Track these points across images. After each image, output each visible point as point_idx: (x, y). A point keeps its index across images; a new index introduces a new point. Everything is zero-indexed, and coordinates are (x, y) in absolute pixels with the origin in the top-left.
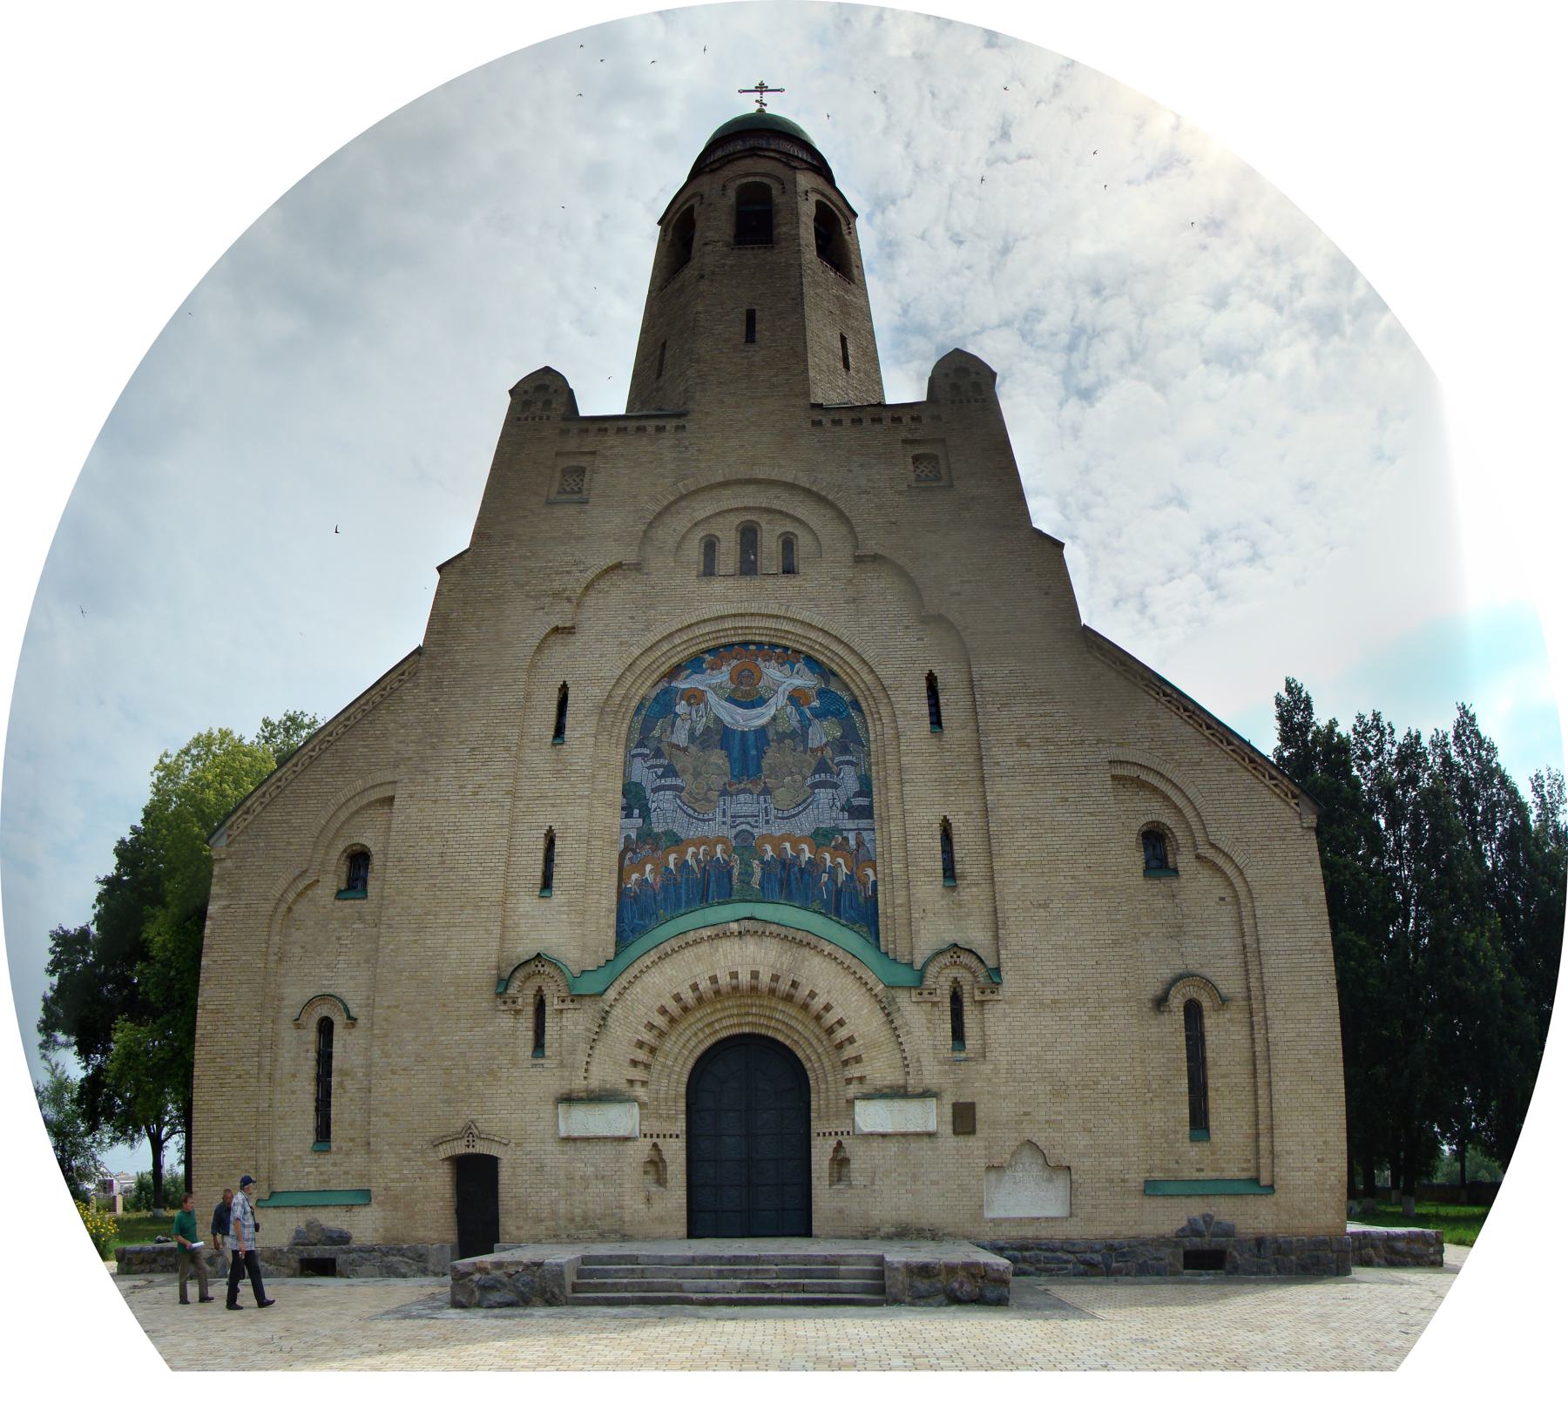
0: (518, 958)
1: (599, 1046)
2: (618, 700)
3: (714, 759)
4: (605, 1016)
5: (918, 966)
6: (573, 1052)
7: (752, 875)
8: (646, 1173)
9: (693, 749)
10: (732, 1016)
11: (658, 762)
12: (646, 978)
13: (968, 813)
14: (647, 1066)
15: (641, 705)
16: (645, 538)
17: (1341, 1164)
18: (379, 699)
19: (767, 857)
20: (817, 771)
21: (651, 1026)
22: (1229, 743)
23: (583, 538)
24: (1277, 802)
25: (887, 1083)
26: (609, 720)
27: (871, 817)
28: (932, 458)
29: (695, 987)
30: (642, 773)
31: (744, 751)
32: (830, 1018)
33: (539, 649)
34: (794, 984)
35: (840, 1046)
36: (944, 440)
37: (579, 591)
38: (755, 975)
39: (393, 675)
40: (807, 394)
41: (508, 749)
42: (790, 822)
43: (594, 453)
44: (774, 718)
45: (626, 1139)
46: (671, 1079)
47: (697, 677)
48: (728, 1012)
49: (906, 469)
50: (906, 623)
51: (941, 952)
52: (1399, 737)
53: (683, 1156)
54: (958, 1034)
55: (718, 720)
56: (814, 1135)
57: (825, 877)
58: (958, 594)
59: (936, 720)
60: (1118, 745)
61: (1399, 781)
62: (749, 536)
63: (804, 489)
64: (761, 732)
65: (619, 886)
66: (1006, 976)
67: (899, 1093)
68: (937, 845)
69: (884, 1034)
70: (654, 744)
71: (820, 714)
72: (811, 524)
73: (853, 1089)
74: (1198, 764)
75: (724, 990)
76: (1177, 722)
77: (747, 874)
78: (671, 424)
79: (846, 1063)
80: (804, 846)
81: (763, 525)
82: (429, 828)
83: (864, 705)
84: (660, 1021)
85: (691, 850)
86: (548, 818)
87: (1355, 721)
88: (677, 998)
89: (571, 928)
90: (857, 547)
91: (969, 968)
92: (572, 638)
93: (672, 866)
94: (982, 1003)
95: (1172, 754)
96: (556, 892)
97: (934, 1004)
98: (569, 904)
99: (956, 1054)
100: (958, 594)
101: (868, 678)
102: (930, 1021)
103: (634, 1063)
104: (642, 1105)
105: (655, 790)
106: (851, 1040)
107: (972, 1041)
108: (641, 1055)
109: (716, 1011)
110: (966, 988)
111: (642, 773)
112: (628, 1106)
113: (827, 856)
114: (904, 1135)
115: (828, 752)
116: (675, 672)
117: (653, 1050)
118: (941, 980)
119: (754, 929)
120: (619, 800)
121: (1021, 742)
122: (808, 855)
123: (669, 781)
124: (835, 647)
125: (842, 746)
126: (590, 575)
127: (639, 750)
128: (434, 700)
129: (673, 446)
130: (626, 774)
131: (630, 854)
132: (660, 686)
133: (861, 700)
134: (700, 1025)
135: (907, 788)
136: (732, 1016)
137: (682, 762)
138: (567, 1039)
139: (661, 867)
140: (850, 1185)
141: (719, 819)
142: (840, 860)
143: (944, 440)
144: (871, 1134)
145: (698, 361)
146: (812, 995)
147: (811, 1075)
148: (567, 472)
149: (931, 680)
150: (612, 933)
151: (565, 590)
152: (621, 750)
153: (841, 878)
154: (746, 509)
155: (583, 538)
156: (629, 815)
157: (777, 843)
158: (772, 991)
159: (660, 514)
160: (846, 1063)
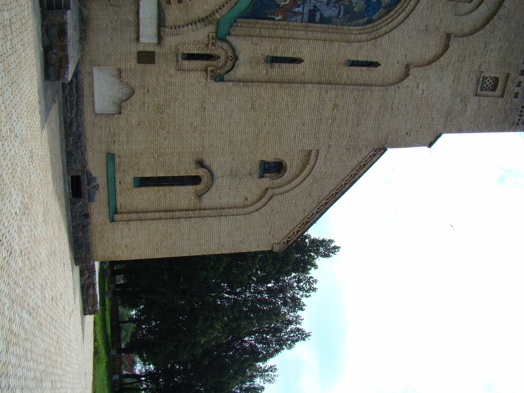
13: (304, 74)
17: (125, 257)
22: (317, 213)
24: (286, 233)
25: (167, 16)
28: (494, 88)
36: (502, 96)
49: (492, 74)
50: (408, 56)
51: (234, 51)
52: (304, 300)
54: (191, 57)
58: (417, 87)
59: (354, 64)
61: (286, 296)
66: (219, 85)
67: (161, 23)
68: (290, 55)
74: (310, 195)
76: (331, 188)
83: (369, 26)
87: (315, 278)
90: (456, 36)
91: (224, 65)
94: (206, 71)
95: (317, 183)
97: (207, 45)
99: (180, 55)
100: (417, 87)
101: (383, 31)
102: (199, 42)
110: (214, 63)
114: (138, 24)
118: (219, 50)
121: (336, 106)
125: (349, 10)
135: (321, 43)
143: (502, 96)
144: (138, 6)
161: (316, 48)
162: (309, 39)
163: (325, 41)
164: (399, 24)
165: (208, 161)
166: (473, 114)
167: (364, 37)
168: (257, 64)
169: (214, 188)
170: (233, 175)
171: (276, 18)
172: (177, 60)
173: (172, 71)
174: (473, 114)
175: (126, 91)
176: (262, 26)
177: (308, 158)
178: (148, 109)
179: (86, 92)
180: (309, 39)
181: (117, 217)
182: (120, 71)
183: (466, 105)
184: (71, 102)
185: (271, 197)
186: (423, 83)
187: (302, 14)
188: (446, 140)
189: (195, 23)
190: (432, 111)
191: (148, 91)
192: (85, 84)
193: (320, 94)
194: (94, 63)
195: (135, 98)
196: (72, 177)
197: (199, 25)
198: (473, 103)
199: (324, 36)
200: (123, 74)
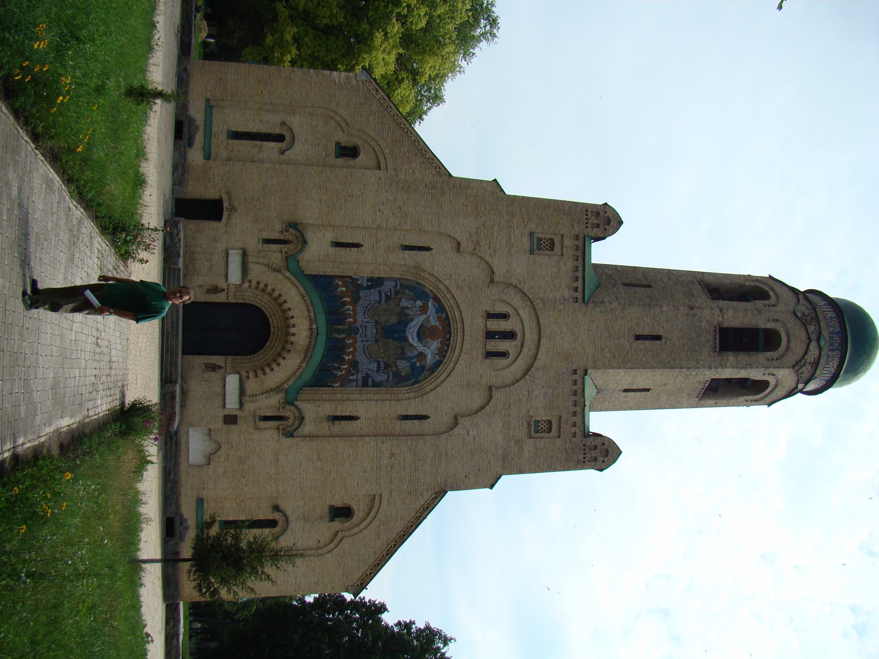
1: (266, 268)
2: (423, 274)
3: (393, 318)
4: (279, 271)
5: (295, 403)
9: (398, 309)
14: (257, 288)
15: (421, 285)
16: (508, 285)
18: (427, 156)
20: (385, 363)
21: (273, 290)
22: (387, 554)
26: (413, 271)
28: (550, 432)
29: (289, 309)
30: (388, 286)
32: (274, 366)
33: (449, 236)
35: (262, 369)
37: (479, 254)
38: (294, 335)
40: (595, 367)
41: (399, 224)
42: (361, 351)
44: (412, 345)
45: (227, 278)
46: (251, 297)
47: (434, 311)
49: (542, 416)
53: (219, 301)
54: (266, 418)
55: (412, 320)
57: (336, 365)
59: (406, 418)
60: (389, 500)
62: (510, 335)
63: (533, 364)
64: (406, 340)
66: (288, 441)
67: (242, 392)
68: (347, 414)
71: (413, 366)
73: (244, 374)
76: (398, 530)
77: (339, 331)
78: (579, 295)
79: (255, 371)
82: (365, 189)
84: (276, 294)
85: (351, 308)
88: (285, 302)
90: (498, 388)
91: (293, 424)
94: (278, 429)
96: (334, 249)
97: (279, 409)
103: (258, 283)
104: (241, 285)
105: (380, 292)
106: (265, 374)
107: (262, 424)
108: (262, 286)
110: (285, 423)
111: (388, 286)
114: (224, 395)
115: (394, 369)
116: (437, 299)
117: (264, 290)
119: (313, 335)
120: (376, 276)
121: (392, 455)
123: (383, 298)
124: (445, 374)
126: (488, 259)
130: (388, 279)
133: (418, 385)
135: (374, 402)
140: (204, 372)
141: (365, 320)
144: (225, 381)
145: (623, 308)
146: (284, 358)
148: (552, 242)
149: (426, 417)
150: (315, 273)
154: (524, 334)
156: (368, 280)
157: (353, 345)
158: (286, 342)
159: (522, 292)
160: (255, 371)
161: (369, 407)
163: (377, 400)
165: (283, 506)
168: (321, 422)
169: (288, 532)
170: (306, 518)
173: (251, 430)
176: (324, 392)
177: (373, 502)
179: (183, 447)
182: (210, 430)
183: (522, 448)
185: (342, 539)
187: (357, 380)
188: (505, 480)
197: (271, 393)
198: (528, 446)
199: (376, 397)
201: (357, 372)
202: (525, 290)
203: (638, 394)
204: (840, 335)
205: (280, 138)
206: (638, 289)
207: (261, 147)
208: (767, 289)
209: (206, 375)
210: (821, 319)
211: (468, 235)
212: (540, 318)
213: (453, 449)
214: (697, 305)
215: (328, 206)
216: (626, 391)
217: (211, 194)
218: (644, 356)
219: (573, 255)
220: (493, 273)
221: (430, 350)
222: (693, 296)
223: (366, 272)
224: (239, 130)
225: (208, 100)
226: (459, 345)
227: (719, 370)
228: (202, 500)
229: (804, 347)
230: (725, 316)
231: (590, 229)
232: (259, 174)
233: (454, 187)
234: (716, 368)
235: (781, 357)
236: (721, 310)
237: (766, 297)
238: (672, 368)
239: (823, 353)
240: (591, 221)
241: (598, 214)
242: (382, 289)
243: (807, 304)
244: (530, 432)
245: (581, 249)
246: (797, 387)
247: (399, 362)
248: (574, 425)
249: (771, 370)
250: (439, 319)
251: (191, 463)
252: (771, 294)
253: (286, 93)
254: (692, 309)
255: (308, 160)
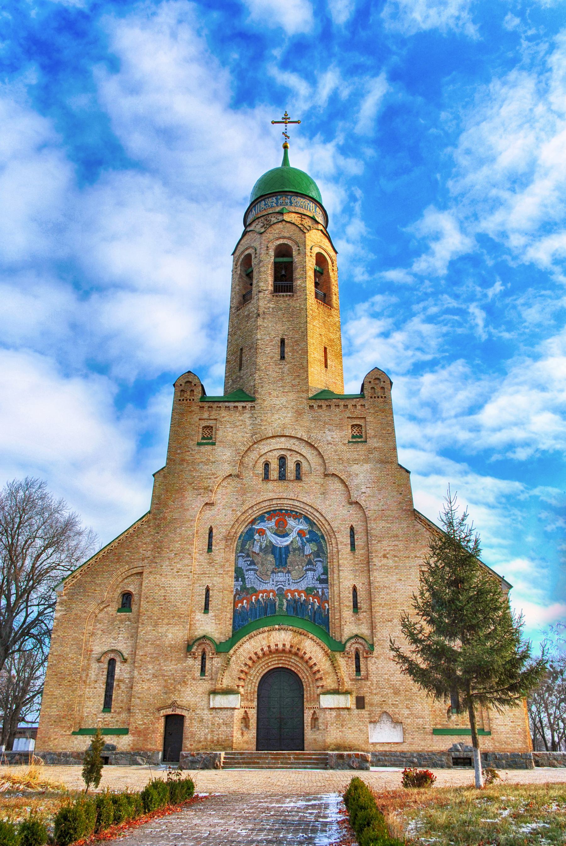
0: (195, 637)
5: (343, 643)
6: (217, 674)
7: (283, 605)
8: (242, 723)
9: (261, 554)
10: (275, 660)
11: (248, 559)
12: (244, 645)
13: (363, 584)
16: (241, 463)
19: (289, 598)
21: (246, 664)
23: (214, 462)
26: (229, 543)
27: (327, 583)
28: (361, 426)
30: (242, 563)
31: (281, 556)
34: (298, 649)
35: (315, 673)
39: (139, 523)
41: (190, 554)
43: (216, 419)
44: (292, 542)
47: (262, 524)
48: (274, 659)
49: (348, 432)
50: (343, 504)
53: (256, 716)
56: (305, 708)
57: (310, 607)
58: (365, 493)
62: (282, 460)
64: (287, 547)
65: (234, 609)
67: (336, 692)
68: (351, 596)
69: (330, 669)
70: (246, 552)
71: (309, 541)
72: (307, 457)
73: (319, 690)
75: (272, 651)
77: (281, 605)
78: (249, 405)
79: (317, 680)
80: (302, 594)
81: (289, 458)
82: (159, 585)
83: (326, 538)
85: (261, 595)
86: (207, 582)
89: (214, 626)
92: (213, 508)
93: (253, 601)
94: (367, 658)
97: (349, 658)
98: (215, 616)
99: (357, 677)
100: (365, 493)
101: (328, 527)
102: (347, 664)
103: (240, 679)
104: (242, 695)
105: (247, 570)
106: (319, 671)
108: (243, 676)
109: (269, 658)
111: (242, 563)
112: (237, 696)
113: (311, 598)
114: (338, 708)
115: (312, 556)
116: (253, 522)
118: (351, 647)
120: (234, 574)
121: (385, 556)
122: (303, 598)
124: (315, 513)
125: (317, 554)
127: (241, 554)
128: (158, 533)
129: (250, 417)
130: (236, 564)
131: (238, 596)
132: (248, 527)
134: (264, 664)
135: (341, 573)
136: (275, 660)
137: (257, 559)
138: (214, 669)
139: (249, 601)
140: (318, 729)
141: (271, 582)
142: (316, 600)
144: (326, 708)
145: (259, 370)
146: (305, 653)
147: (304, 684)
148: (205, 427)
149: (352, 529)
150: (231, 627)
151: (209, 486)
152: (234, 554)
153: (316, 607)
155: (214, 462)
156: (237, 580)
157: (292, 592)
158: (290, 651)
160: (317, 680)
162: (339, 582)
163: (339, 571)
164: (322, 515)
166: (380, 440)
167: (333, 541)
168: (359, 620)
171: (327, 607)
172: (361, 679)
173: (369, 683)
174: (380, 440)
175: (385, 717)
178: (397, 701)
179: (387, 748)
180: (339, 582)
181: (487, 729)
182: (371, 722)
184: (395, 761)
186: (361, 489)
187: (323, 589)
189: (335, 667)
190: (382, 476)
191: (384, 701)
192: (381, 749)
193: (376, 569)
194: (367, 742)
195: (389, 711)
196: (454, 765)
198: (373, 443)
200: (373, 720)
201: (315, 588)
202: (245, 449)
203: (329, 356)
204: (279, 197)
205: (112, 663)
206: (244, 359)
207: (119, 681)
208: (243, 256)
209: (322, 727)
210: (266, 213)
211: (199, 497)
212: (267, 436)
213: (378, 505)
214: (255, 312)
215: (173, 617)
216: (326, 366)
217: (161, 726)
218: (297, 352)
219: (216, 410)
220: (231, 475)
221: (295, 526)
222: (249, 315)
223: (230, 582)
224: (103, 702)
225: (74, 733)
226: (291, 502)
227: (308, 292)
228: (434, 730)
229: (288, 225)
230: (265, 288)
231: (195, 398)
232: (143, 681)
233: (158, 509)
234: (306, 295)
235: (297, 244)
236: (260, 292)
237: (249, 256)
238: (307, 329)
239: (294, 211)
240: (188, 397)
241: (182, 391)
242: (244, 569)
243: (254, 225)
244: (361, 442)
245: (211, 404)
246: (321, 231)
247: (307, 553)
248: (355, 406)
249: (308, 251)
250: (270, 519)
251: (401, 741)
252: (247, 253)
253: (72, 659)
254: (259, 315)
255: (131, 637)
